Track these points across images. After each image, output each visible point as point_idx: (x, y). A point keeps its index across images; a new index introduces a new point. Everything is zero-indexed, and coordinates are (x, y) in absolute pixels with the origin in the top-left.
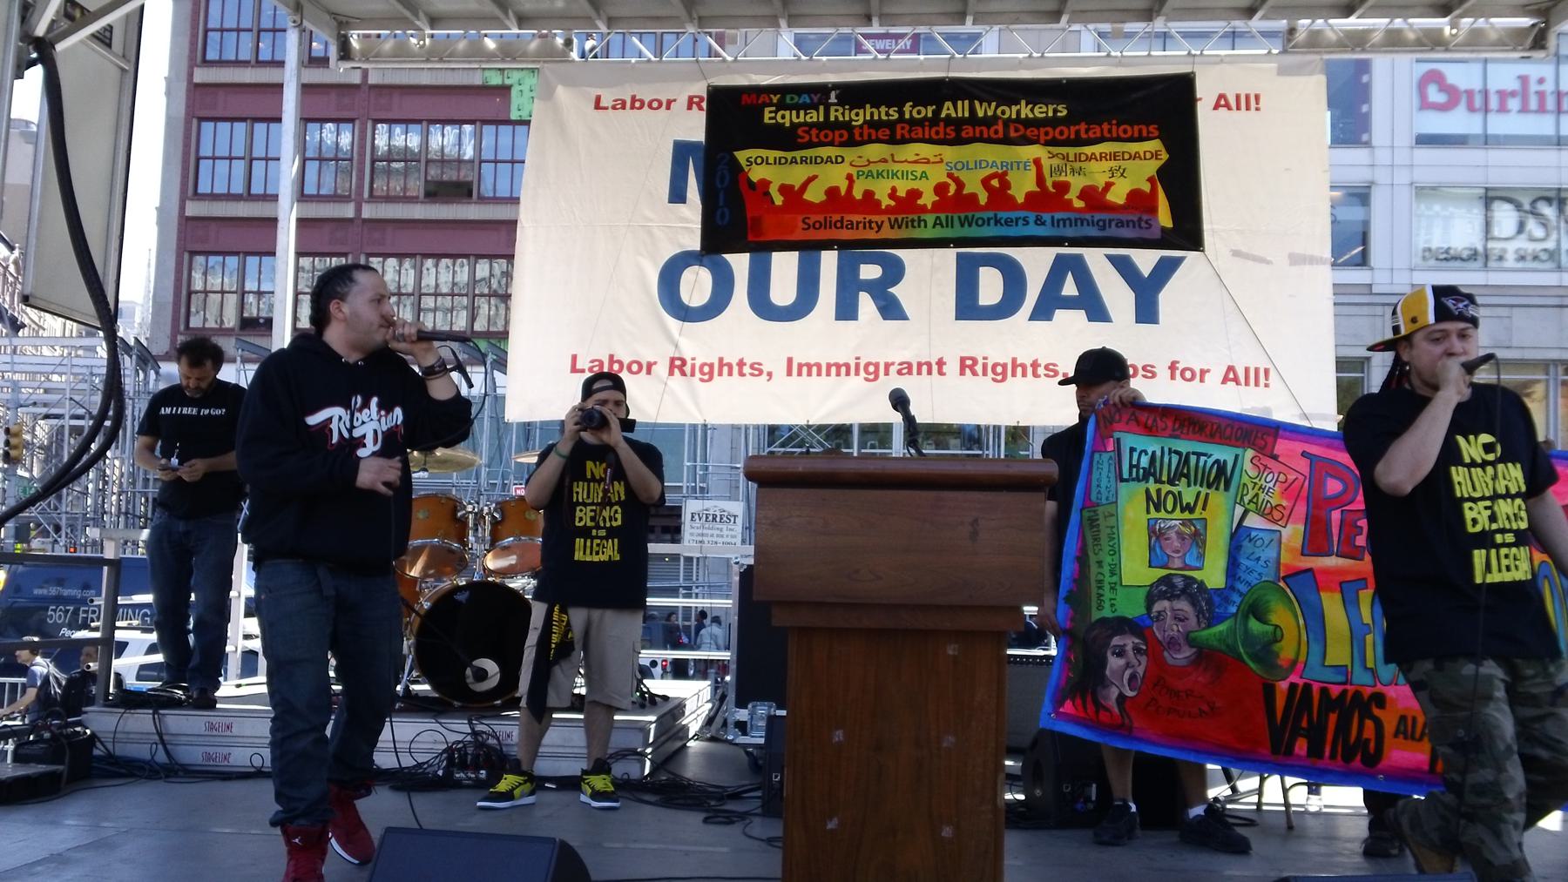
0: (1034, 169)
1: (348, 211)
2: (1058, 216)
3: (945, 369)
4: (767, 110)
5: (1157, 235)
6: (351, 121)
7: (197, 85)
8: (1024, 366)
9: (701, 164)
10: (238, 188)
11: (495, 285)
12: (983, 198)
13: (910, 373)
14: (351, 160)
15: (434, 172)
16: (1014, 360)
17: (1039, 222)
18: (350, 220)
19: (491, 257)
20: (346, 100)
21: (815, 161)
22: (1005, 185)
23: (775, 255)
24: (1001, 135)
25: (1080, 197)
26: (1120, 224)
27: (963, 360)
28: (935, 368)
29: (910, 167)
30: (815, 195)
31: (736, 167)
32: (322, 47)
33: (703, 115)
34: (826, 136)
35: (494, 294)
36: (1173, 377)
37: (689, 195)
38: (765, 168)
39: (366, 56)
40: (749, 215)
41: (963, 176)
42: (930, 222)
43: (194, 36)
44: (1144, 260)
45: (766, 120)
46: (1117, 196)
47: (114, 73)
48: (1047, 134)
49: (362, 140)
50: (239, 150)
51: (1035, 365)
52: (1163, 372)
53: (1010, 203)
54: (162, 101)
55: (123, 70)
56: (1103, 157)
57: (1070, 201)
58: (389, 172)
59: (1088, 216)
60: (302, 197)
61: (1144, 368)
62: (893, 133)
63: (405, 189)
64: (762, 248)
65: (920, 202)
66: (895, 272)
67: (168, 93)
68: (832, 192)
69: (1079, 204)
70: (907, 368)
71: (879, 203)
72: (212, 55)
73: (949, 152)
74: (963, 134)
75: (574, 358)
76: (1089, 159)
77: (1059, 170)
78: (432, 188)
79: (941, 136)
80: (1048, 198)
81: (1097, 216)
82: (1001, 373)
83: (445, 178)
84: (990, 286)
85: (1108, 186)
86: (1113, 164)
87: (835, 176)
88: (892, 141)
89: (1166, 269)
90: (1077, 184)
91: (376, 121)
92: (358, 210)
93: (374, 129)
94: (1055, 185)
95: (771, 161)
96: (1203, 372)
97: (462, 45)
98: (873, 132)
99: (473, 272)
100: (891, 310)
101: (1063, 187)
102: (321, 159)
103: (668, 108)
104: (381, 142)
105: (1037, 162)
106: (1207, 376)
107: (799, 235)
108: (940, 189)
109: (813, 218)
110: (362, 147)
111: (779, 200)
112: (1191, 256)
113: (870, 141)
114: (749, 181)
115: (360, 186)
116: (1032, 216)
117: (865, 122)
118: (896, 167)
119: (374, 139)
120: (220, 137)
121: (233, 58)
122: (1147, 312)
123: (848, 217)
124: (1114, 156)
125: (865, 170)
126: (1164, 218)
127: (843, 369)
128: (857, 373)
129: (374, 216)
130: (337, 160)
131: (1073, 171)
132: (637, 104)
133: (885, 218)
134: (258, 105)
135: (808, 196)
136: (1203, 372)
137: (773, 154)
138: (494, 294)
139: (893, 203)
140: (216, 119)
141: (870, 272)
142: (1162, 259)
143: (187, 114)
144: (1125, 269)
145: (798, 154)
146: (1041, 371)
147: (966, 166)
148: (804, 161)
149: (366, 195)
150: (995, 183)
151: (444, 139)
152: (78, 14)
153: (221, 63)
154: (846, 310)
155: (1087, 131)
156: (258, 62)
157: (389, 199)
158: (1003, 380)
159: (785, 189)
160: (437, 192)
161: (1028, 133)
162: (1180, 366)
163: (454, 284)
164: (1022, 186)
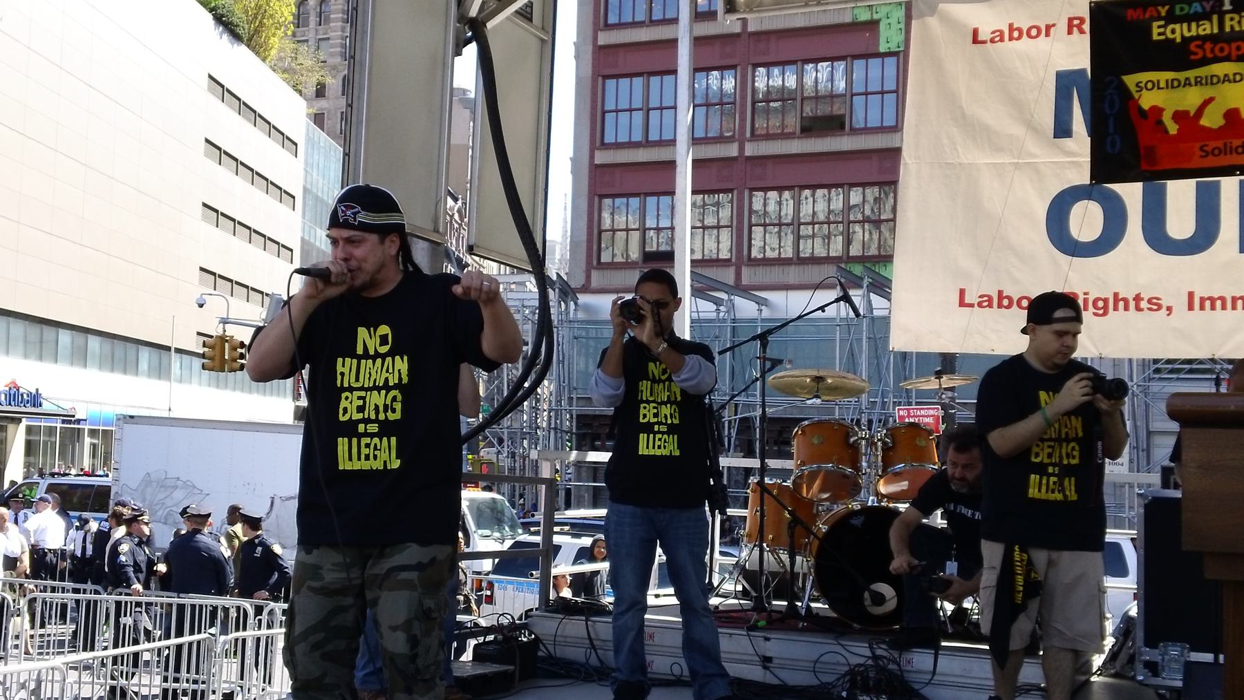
1: (732, 150)
4: (1155, 24)
6: (733, 67)
7: (601, 47)
10: (637, 136)
11: (868, 212)
14: (734, 103)
15: (808, 111)
19: (864, 185)
34: (1222, 50)
35: (866, 220)
45: (1155, 37)
49: (744, 84)
50: (637, 103)
54: (572, 63)
58: (767, 111)
60: (695, 141)
63: (783, 126)
67: (577, 57)
83: (819, 113)
92: (742, 149)
99: (847, 199)
102: (708, 105)
103: (1047, 35)
104: (761, 84)
115: (742, 127)
119: (754, 81)
120: (622, 92)
132: (1016, 34)
134: (654, 60)
137: (1164, 76)
138: (866, 220)
143: (593, 73)
149: (748, 135)
151: (819, 76)
156: (651, 21)
157: (769, 137)
160: (811, 127)
163: (830, 212)
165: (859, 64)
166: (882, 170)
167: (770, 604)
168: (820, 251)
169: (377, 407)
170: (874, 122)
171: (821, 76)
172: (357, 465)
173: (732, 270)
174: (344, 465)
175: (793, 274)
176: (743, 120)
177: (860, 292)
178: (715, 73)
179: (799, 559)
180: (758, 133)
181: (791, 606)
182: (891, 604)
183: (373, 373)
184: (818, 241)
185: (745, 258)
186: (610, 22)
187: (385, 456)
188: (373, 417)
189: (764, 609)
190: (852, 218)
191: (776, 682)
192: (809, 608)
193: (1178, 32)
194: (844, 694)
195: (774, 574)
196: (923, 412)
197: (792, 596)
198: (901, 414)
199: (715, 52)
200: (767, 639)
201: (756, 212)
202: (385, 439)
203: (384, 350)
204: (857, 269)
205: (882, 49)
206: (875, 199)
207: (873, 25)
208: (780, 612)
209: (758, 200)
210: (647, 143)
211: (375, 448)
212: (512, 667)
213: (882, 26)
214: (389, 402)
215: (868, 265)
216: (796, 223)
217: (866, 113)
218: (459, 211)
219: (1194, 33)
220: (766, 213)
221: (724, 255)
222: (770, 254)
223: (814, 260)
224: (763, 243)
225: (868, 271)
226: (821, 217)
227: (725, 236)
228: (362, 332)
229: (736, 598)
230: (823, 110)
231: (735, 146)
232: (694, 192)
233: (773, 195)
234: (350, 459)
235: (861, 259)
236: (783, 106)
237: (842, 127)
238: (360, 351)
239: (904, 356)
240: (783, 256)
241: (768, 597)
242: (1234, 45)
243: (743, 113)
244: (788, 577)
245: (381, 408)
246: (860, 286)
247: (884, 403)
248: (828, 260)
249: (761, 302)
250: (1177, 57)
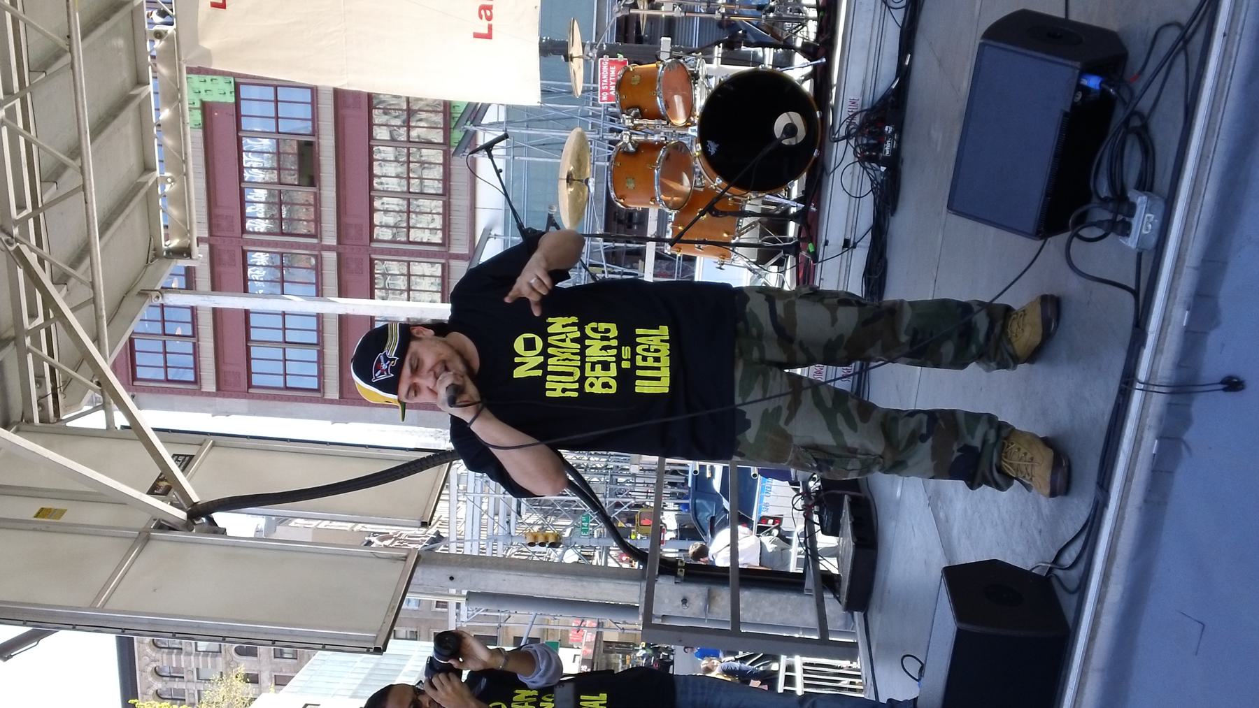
1: (330, 258)
6: (244, 253)
7: (218, 389)
11: (398, 122)
14: (282, 255)
15: (292, 178)
18: (339, 255)
19: (371, 125)
20: (225, 257)
32: (176, 279)
39: (186, 233)
43: (172, 391)
47: (216, 453)
54: (234, 418)
55: (213, 445)
58: (291, 220)
67: (228, 414)
72: (190, 376)
78: (306, 180)
91: (244, 230)
92: (329, 248)
93: (250, 233)
97: (169, 142)
99: (384, 143)
102: (283, 281)
110: (269, 244)
115: (306, 246)
119: (259, 233)
120: (265, 369)
121: (191, 358)
129: (335, 234)
130: (282, 267)
138: (407, 125)
140: (249, 373)
143: (245, 397)
149: (315, 241)
152: (164, 484)
153: (196, 368)
156: (193, 336)
157: (318, 220)
160: (309, 176)
163: (396, 161)
166: (355, 109)
167: (791, 239)
168: (438, 172)
169: (605, 348)
170: (306, 112)
171: (257, 162)
172: (665, 373)
173: (453, 263)
174: (663, 387)
175: (460, 201)
176: (299, 246)
177: (480, 134)
178: (250, 271)
179: (748, 208)
180: (313, 231)
181: (795, 217)
182: (795, 118)
183: (565, 356)
184: (426, 174)
185: (442, 249)
186: (190, 333)
187: (656, 341)
188: (614, 352)
189: (797, 245)
190: (404, 138)
191: (869, 236)
192: (798, 200)
194: (883, 169)
195: (763, 233)
196: (605, 77)
197: (785, 217)
198: (607, 96)
199: (228, 269)
200: (826, 243)
201: (394, 235)
202: (638, 340)
203: (539, 343)
204: (457, 135)
205: (232, 99)
206: (385, 114)
207: (206, 108)
208: (800, 229)
209: (383, 234)
210: (320, 345)
211: (647, 350)
212: (846, 498)
213: (208, 98)
214: (598, 336)
215: (453, 124)
216: (408, 195)
217: (296, 120)
218: (382, 540)
220: (396, 226)
221: (438, 270)
222: (438, 222)
223: (446, 179)
224: (427, 229)
225: (459, 125)
227: (417, 268)
228: (519, 373)
229: (784, 272)
230: (291, 163)
231: (326, 254)
232: (372, 297)
233: (378, 218)
234: (658, 379)
235: (447, 130)
236: (286, 204)
237: (310, 144)
238: (539, 373)
239: (545, 92)
240: (441, 210)
241: (784, 240)
243: (292, 245)
244: (765, 219)
245: (606, 343)
246: (475, 133)
247: (594, 116)
248: (446, 165)
249: (487, 235)
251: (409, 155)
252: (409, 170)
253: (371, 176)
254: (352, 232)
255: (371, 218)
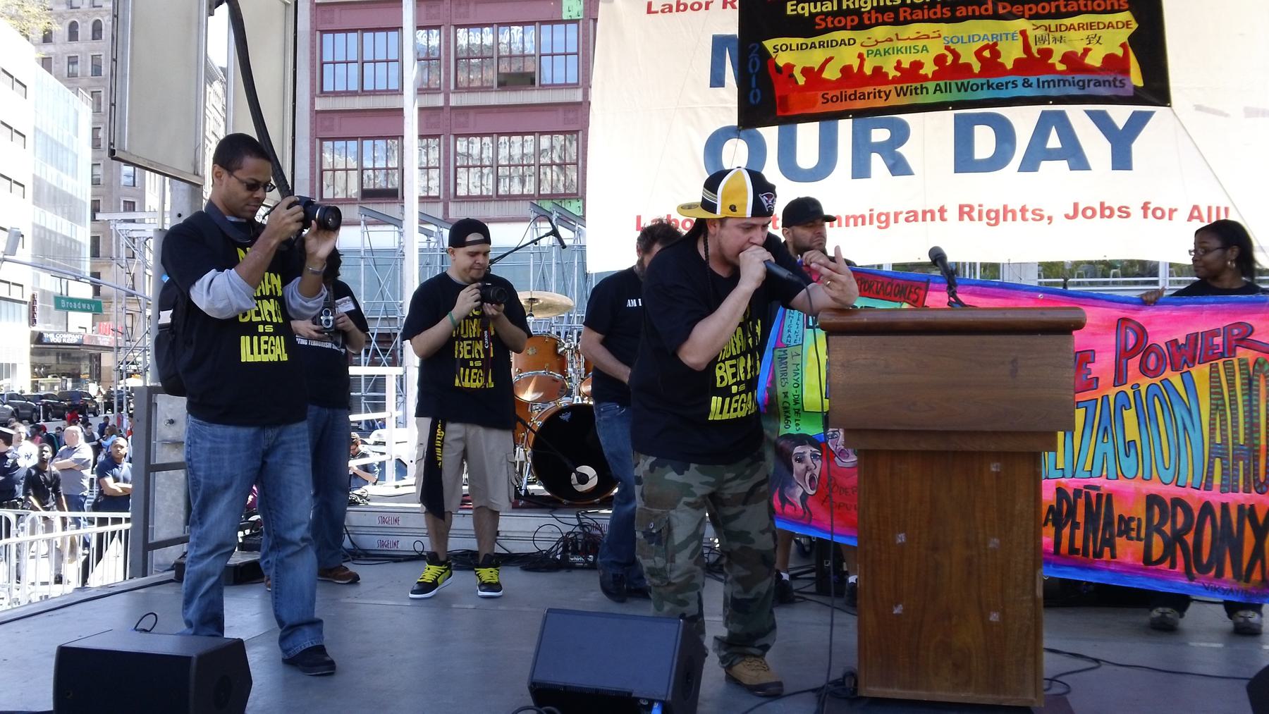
0: (1020, 38)
2: (1043, 78)
3: (946, 215)
5: (1130, 93)
8: (1013, 212)
9: (736, 53)
12: (977, 67)
13: (916, 220)
16: (1005, 207)
17: (1027, 84)
21: (831, 44)
22: (996, 54)
23: (800, 126)
24: (990, 12)
25: (1061, 62)
26: (1097, 84)
27: (961, 207)
28: (937, 215)
29: (913, 43)
30: (832, 73)
31: (765, 54)
33: (737, 11)
34: (840, 22)
36: (1145, 216)
37: (726, 81)
38: (788, 53)
40: (777, 94)
41: (959, 48)
42: (931, 90)
44: (1120, 114)
45: (789, 12)
46: (1094, 60)
48: (1030, 9)
51: (1023, 210)
52: (1137, 212)
53: (999, 70)
56: (1080, 27)
57: (1053, 65)
59: (1069, 77)
61: (1120, 209)
62: (897, 16)
64: (788, 120)
65: (922, 72)
66: (901, 134)
68: (846, 70)
69: (1061, 67)
70: (913, 216)
71: (886, 75)
73: (946, 29)
74: (958, 14)
75: (639, 218)
76: (1069, 29)
77: (1043, 40)
79: (939, 15)
80: (1034, 63)
81: (1078, 77)
82: (995, 217)
84: (984, 141)
85: (1086, 51)
86: (1090, 32)
87: (848, 56)
88: (897, 22)
89: (1138, 123)
90: (1059, 50)
94: (1039, 51)
95: (794, 47)
96: (1172, 211)
98: (880, 16)
100: (898, 167)
101: (1047, 53)
103: (707, 8)
105: (1023, 33)
106: (1175, 214)
107: (820, 108)
108: (939, 60)
109: (831, 93)
111: (801, 80)
112: (1159, 111)
113: (877, 24)
114: (776, 65)
116: (1019, 80)
117: (873, 8)
118: (900, 44)
122: (1122, 160)
123: (860, 90)
124: (1090, 26)
125: (874, 49)
126: (1136, 78)
127: (860, 220)
128: (871, 223)
131: (1055, 39)
133: (891, 87)
135: (826, 75)
136: (1172, 211)
139: (898, 74)
141: (880, 135)
142: (1134, 113)
144: (1103, 122)
145: (816, 40)
146: (1029, 215)
147: (961, 40)
148: (821, 45)
150: (987, 54)
154: (861, 170)
155: (1066, 6)
158: (997, 224)
159: (806, 71)
161: (1014, 10)
162: (1152, 206)
164: (1011, 53)
165: (546, 29)
166: (572, 119)
168: (516, 189)
170: (559, 79)
190: (543, 161)
193: (806, 9)
209: (462, 145)
216: (495, 166)
217: (553, 71)
219: (819, 10)
220: (469, 156)
222: (475, 192)
223: (511, 198)
226: (516, 160)
235: (551, 197)
240: (485, 193)
242: (849, 19)
250: (806, 28)
251: (529, 165)
252: (516, 166)
253: (510, 134)
254: (462, 119)
255: (476, 135)
